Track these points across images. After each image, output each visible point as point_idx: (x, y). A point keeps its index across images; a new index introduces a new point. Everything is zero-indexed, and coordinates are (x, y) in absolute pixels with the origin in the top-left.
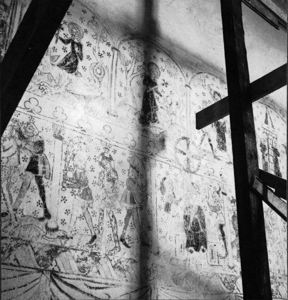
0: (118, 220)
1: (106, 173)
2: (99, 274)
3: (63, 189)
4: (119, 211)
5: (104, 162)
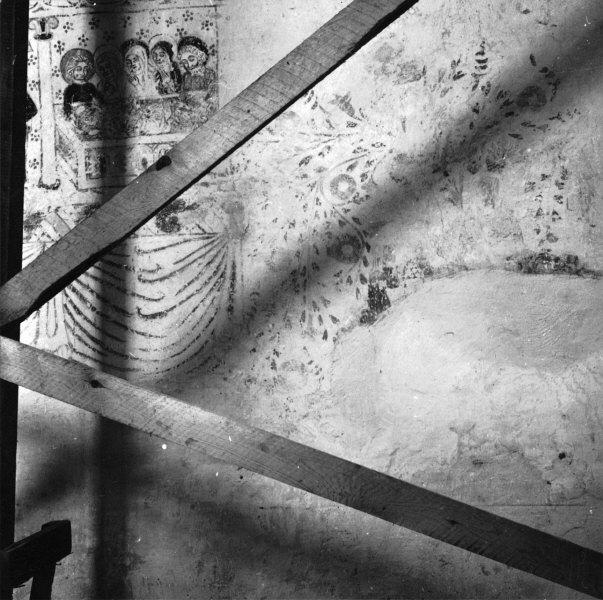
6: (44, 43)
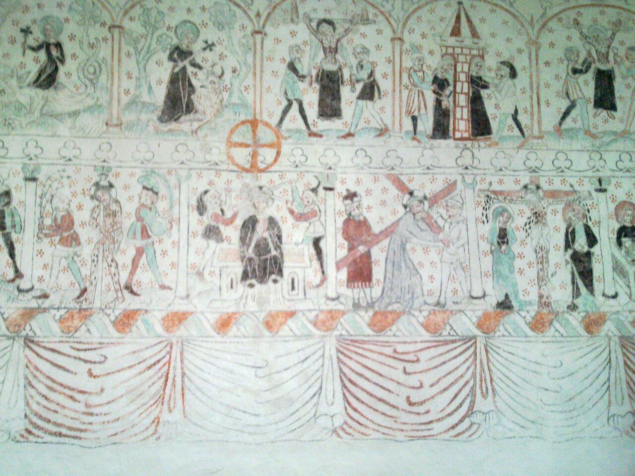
0: (120, 264)
1: (102, 207)
2: (90, 332)
3: (40, 241)
4: (124, 252)
5: (99, 193)
6: (601, 195)
